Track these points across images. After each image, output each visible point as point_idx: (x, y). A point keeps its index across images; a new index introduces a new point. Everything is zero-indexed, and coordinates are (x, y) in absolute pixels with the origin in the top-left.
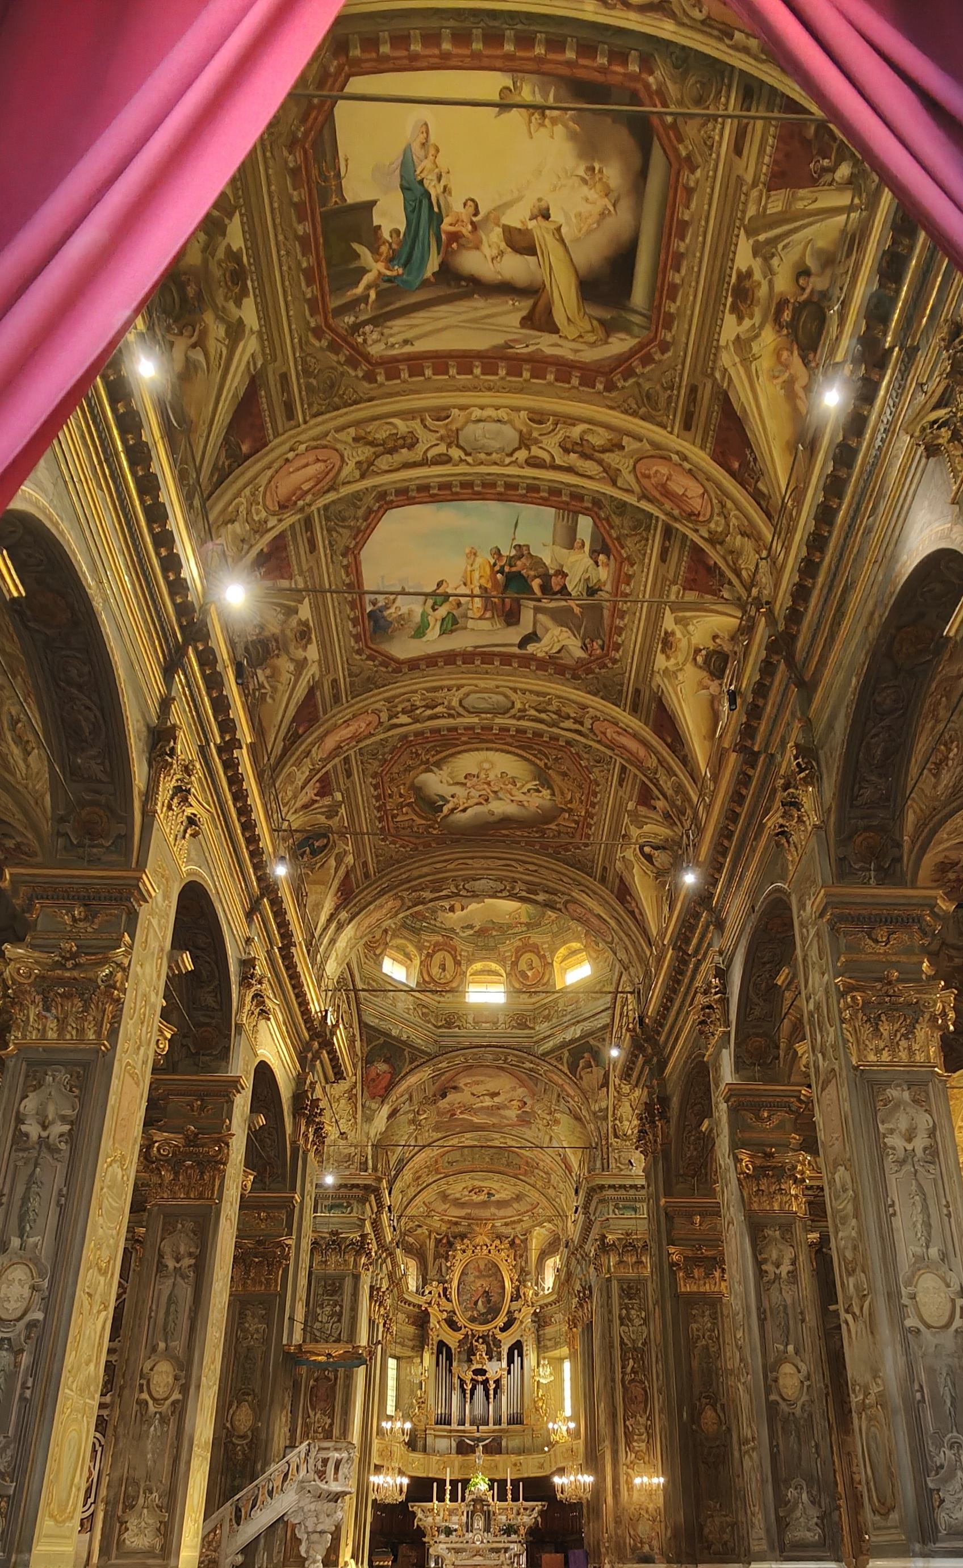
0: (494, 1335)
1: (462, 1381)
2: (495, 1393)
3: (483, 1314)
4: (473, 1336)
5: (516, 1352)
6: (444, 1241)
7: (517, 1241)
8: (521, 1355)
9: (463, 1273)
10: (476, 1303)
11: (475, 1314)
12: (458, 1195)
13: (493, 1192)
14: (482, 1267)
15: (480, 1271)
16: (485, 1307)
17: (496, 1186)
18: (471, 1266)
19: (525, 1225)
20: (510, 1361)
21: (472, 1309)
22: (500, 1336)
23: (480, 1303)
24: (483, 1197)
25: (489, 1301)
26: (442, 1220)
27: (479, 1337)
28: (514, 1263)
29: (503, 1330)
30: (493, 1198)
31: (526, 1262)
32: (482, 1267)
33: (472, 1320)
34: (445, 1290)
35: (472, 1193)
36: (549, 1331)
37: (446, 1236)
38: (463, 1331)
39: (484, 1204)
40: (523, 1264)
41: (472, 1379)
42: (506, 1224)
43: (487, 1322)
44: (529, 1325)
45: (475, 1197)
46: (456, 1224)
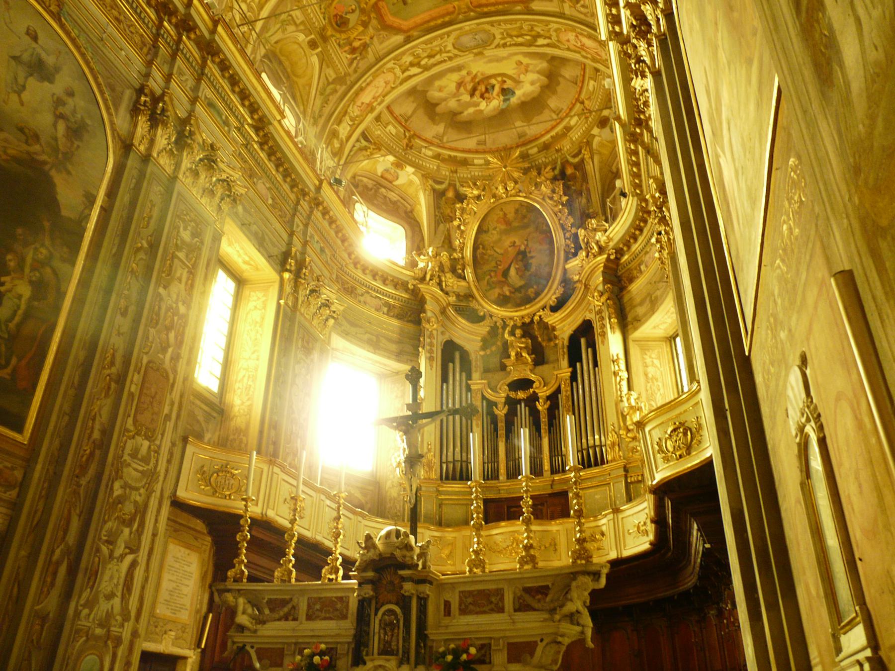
0: (542, 323)
1: (491, 404)
2: (551, 425)
3: (518, 290)
4: (505, 326)
5: (583, 341)
6: (450, 194)
7: (569, 171)
8: (592, 344)
9: (480, 231)
10: (506, 273)
11: (506, 291)
12: (452, 104)
13: (509, 84)
14: (511, 216)
15: (508, 223)
16: (521, 277)
17: (509, 68)
18: (494, 217)
19: (575, 135)
20: (574, 357)
21: (502, 284)
22: (552, 319)
23: (513, 272)
24: (495, 103)
25: (527, 266)
26: (437, 156)
27: (515, 327)
28: (565, 199)
29: (554, 309)
30: (514, 100)
31: (589, 200)
32: (511, 216)
33: (502, 301)
34: (454, 262)
35: (476, 98)
36: (636, 288)
37: (452, 185)
38: (488, 322)
39: (501, 117)
40: (584, 201)
41: (508, 398)
42: (546, 147)
43: (528, 300)
44: (601, 288)
45: (483, 105)
46: (465, 163)
